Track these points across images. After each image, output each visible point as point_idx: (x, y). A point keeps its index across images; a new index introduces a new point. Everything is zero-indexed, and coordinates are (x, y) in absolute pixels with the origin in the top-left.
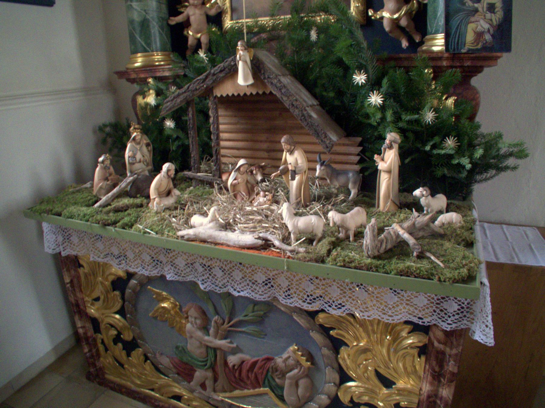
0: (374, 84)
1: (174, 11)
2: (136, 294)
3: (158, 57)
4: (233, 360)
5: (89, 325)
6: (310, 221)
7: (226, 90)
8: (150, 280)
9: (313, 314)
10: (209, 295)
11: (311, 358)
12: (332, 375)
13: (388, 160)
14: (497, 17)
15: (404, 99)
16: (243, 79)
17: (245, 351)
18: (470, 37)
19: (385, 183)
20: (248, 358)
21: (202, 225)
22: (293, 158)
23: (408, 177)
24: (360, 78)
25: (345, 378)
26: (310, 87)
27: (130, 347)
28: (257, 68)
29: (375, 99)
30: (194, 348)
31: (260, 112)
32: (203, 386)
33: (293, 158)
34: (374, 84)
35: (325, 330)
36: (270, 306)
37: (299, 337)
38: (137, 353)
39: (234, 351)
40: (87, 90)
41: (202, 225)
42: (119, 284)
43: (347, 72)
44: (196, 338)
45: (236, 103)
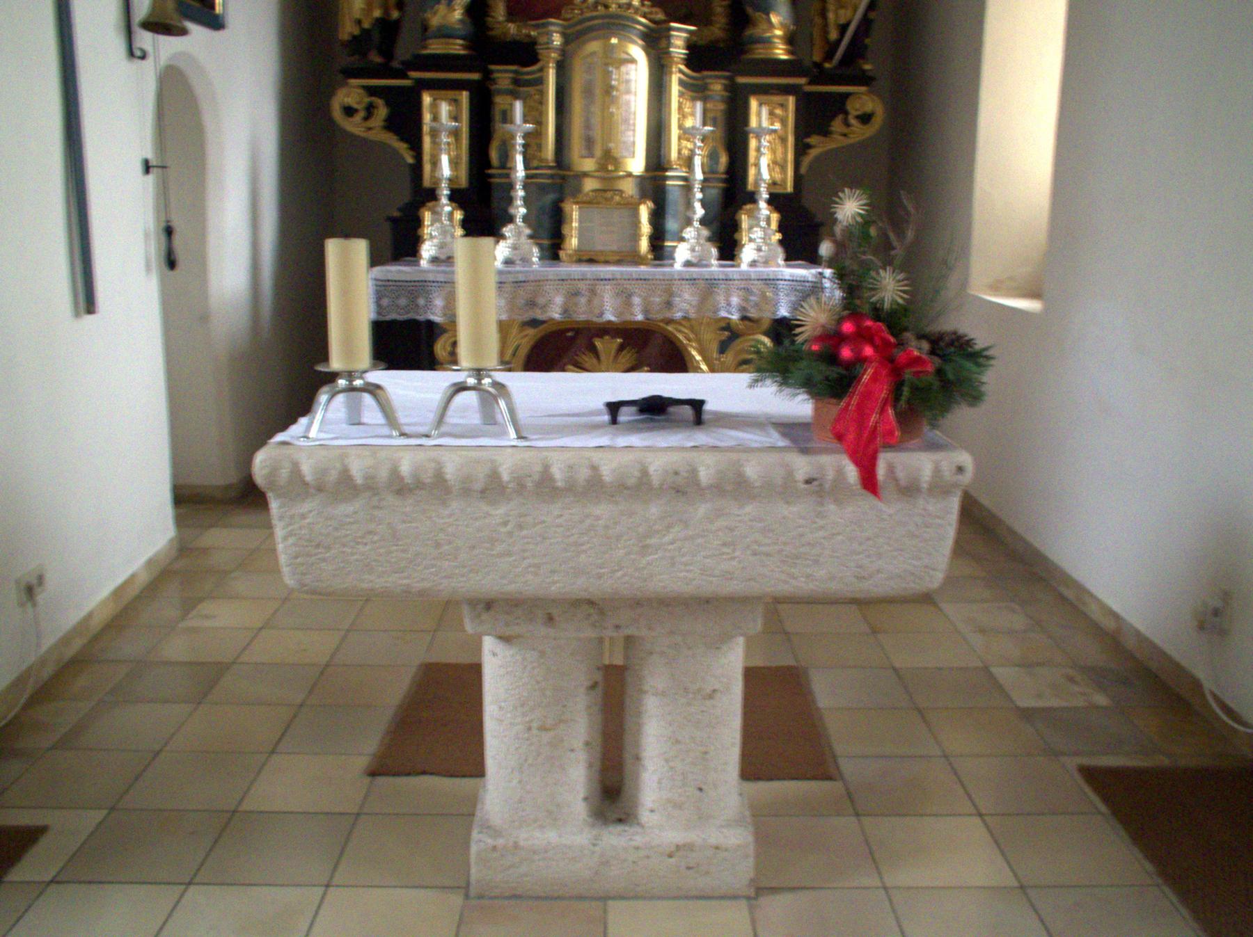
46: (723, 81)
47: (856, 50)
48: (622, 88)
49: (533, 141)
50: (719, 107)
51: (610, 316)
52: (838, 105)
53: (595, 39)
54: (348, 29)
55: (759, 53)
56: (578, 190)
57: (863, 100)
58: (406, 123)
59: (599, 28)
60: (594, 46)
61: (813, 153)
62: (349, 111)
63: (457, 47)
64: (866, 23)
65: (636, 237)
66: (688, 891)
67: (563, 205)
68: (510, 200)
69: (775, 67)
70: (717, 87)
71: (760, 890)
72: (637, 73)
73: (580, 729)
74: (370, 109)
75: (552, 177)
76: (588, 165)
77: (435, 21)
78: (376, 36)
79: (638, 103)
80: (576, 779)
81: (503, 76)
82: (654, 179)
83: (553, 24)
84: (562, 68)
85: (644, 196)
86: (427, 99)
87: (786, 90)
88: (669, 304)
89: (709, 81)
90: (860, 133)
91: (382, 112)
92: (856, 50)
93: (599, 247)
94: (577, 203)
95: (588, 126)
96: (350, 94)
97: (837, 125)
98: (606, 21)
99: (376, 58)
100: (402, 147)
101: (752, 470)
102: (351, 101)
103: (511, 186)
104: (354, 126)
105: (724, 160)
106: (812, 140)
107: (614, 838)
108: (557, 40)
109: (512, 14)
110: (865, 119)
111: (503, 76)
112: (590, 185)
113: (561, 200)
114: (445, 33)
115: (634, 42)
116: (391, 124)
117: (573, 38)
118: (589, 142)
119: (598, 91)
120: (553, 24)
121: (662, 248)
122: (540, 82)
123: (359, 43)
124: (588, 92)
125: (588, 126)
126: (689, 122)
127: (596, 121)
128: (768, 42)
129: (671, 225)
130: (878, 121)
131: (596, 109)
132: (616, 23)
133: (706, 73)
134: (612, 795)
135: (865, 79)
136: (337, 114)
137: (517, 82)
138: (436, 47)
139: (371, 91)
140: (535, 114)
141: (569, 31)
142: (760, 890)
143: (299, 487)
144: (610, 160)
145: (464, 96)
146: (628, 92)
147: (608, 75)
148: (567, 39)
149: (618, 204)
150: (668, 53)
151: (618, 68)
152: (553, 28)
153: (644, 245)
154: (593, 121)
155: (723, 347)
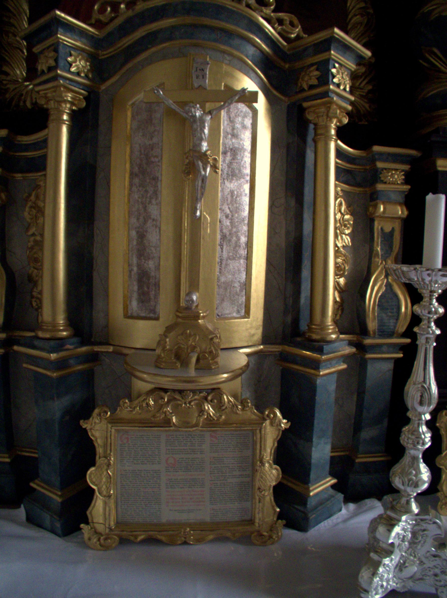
46: (406, 167)
48: (222, 163)
53: (164, 56)
59: (170, 34)
65: (248, 488)
67: (85, 425)
72: (251, 137)
75: (61, 364)
76: (142, 334)
82: (284, 357)
83: (70, 28)
84: (86, 124)
89: (380, 165)
93: (168, 514)
94: (113, 421)
95: (142, 250)
98: (189, 20)
113: (85, 410)
115: (248, 71)
118: (145, 284)
119: (166, 173)
120: (70, 28)
121: (303, 499)
124: (144, 173)
125: (142, 250)
127: (161, 239)
131: (163, 210)
133: (376, 148)
141: (104, 54)
144: (191, 343)
146: (234, 174)
147: (188, 128)
148: (100, 69)
149: (211, 423)
150: (326, 94)
151: (214, 113)
152: (65, 39)
154: (152, 237)
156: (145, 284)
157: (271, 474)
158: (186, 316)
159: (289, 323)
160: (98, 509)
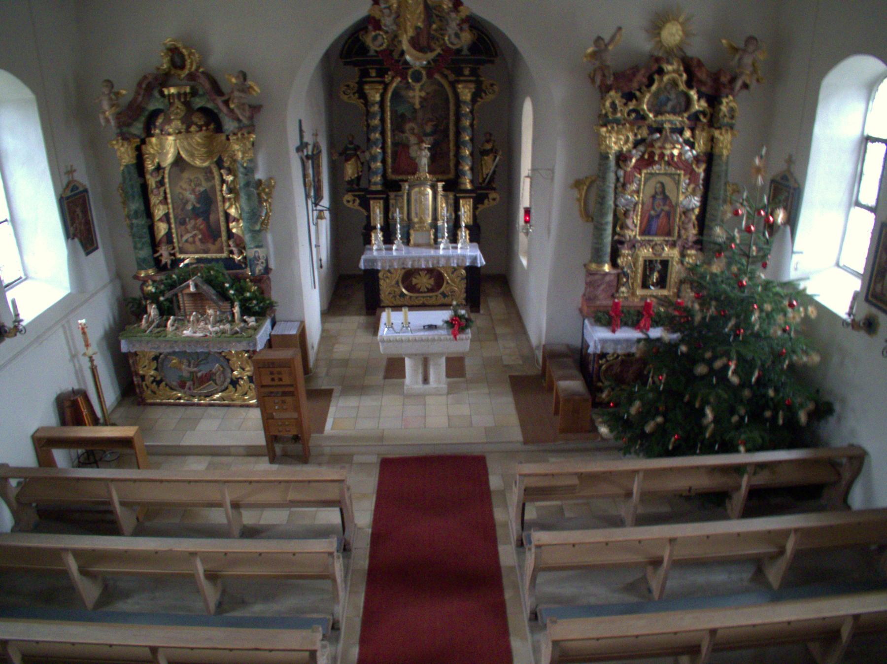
0: (231, 287)
1: (155, 251)
2: (163, 360)
3: (151, 272)
4: (199, 374)
5: (140, 379)
6: (216, 328)
7: (187, 291)
8: (169, 354)
9: (220, 353)
10: (191, 354)
11: (222, 367)
12: (229, 371)
13: (237, 310)
14: (264, 265)
15: (241, 291)
16: (192, 289)
17: (202, 371)
18: (257, 271)
19: (237, 316)
20: (204, 372)
21: (187, 333)
22: (210, 312)
23: (243, 313)
24: (227, 285)
25: (233, 371)
26: (214, 287)
27: (159, 383)
28: (196, 286)
29: (232, 292)
30: (185, 374)
31: (198, 298)
32: (190, 389)
33: (210, 312)
34: (231, 287)
35: (224, 357)
36: (209, 353)
37: (218, 361)
38: (163, 384)
39: (200, 371)
40: (111, 281)
41: (187, 333)
42: (156, 358)
43: (223, 283)
44: (186, 370)
45: (192, 295)
47: (492, 180)
49: (402, 220)
50: (451, 201)
51: (423, 266)
52: (486, 196)
54: (347, 179)
55: (463, 187)
56: (413, 227)
57: (493, 195)
58: (365, 205)
60: (416, 189)
61: (479, 210)
62: (348, 201)
63: (379, 188)
64: (494, 172)
65: (429, 239)
66: (437, 393)
68: (396, 234)
69: (467, 191)
70: (451, 196)
71: (448, 393)
73: (420, 370)
74: (354, 201)
76: (416, 220)
77: (373, 180)
78: (355, 182)
79: (428, 199)
80: (420, 378)
81: (392, 195)
85: (431, 227)
86: (371, 202)
87: (470, 197)
88: (438, 263)
90: (492, 203)
91: (358, 201)
92: (492, 180)
96: (348, 197)
97: (486, 201)
99: (355, 186)
100: (364, 211)
101: (442, 338)
102: (349, 199)
103: (396, 230)
104: (350, 205)
105: (453, 216)
106: (479, 206)
107: (426, 387)
108: (407, 187)
109: (393, 172)
110: (494, 199)
111: (392, 195)
112: (417, 226)
114: (376, 184)
116: (360, 205)
117: (411, 187)
122: (402, 196)
123: (350, 182)
126: (444, 210)
128: (465, 184)
129: (439, 235)
130: (498, 200)
132: (422, 183)
134: (426, 380)
135: (494, 189)
136: (345, 202)
137: (396, 196)
138: (373, 188)
139: (355, 196)
140: (401, 209)
142: (448, 393)
143: (383, 341)
144: (422, 221)
145: (382, 202)
148: (410, 186)
153: (432, 241)
155: (453, 273)
156: (416, 214)
157: (432, 237)
158: (421, 218)
159: (435, 219)
160: (412, 242)
